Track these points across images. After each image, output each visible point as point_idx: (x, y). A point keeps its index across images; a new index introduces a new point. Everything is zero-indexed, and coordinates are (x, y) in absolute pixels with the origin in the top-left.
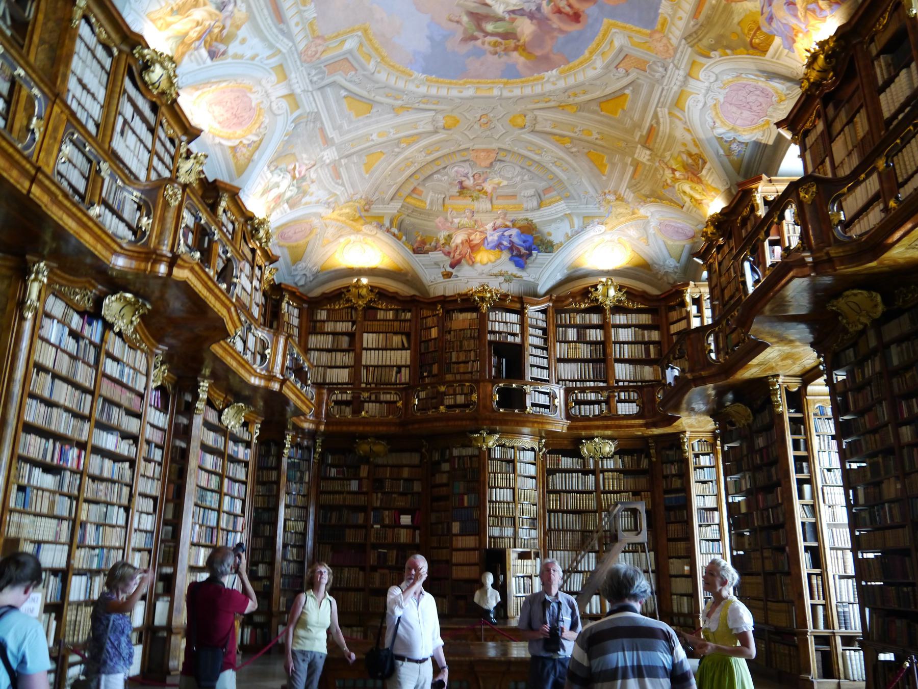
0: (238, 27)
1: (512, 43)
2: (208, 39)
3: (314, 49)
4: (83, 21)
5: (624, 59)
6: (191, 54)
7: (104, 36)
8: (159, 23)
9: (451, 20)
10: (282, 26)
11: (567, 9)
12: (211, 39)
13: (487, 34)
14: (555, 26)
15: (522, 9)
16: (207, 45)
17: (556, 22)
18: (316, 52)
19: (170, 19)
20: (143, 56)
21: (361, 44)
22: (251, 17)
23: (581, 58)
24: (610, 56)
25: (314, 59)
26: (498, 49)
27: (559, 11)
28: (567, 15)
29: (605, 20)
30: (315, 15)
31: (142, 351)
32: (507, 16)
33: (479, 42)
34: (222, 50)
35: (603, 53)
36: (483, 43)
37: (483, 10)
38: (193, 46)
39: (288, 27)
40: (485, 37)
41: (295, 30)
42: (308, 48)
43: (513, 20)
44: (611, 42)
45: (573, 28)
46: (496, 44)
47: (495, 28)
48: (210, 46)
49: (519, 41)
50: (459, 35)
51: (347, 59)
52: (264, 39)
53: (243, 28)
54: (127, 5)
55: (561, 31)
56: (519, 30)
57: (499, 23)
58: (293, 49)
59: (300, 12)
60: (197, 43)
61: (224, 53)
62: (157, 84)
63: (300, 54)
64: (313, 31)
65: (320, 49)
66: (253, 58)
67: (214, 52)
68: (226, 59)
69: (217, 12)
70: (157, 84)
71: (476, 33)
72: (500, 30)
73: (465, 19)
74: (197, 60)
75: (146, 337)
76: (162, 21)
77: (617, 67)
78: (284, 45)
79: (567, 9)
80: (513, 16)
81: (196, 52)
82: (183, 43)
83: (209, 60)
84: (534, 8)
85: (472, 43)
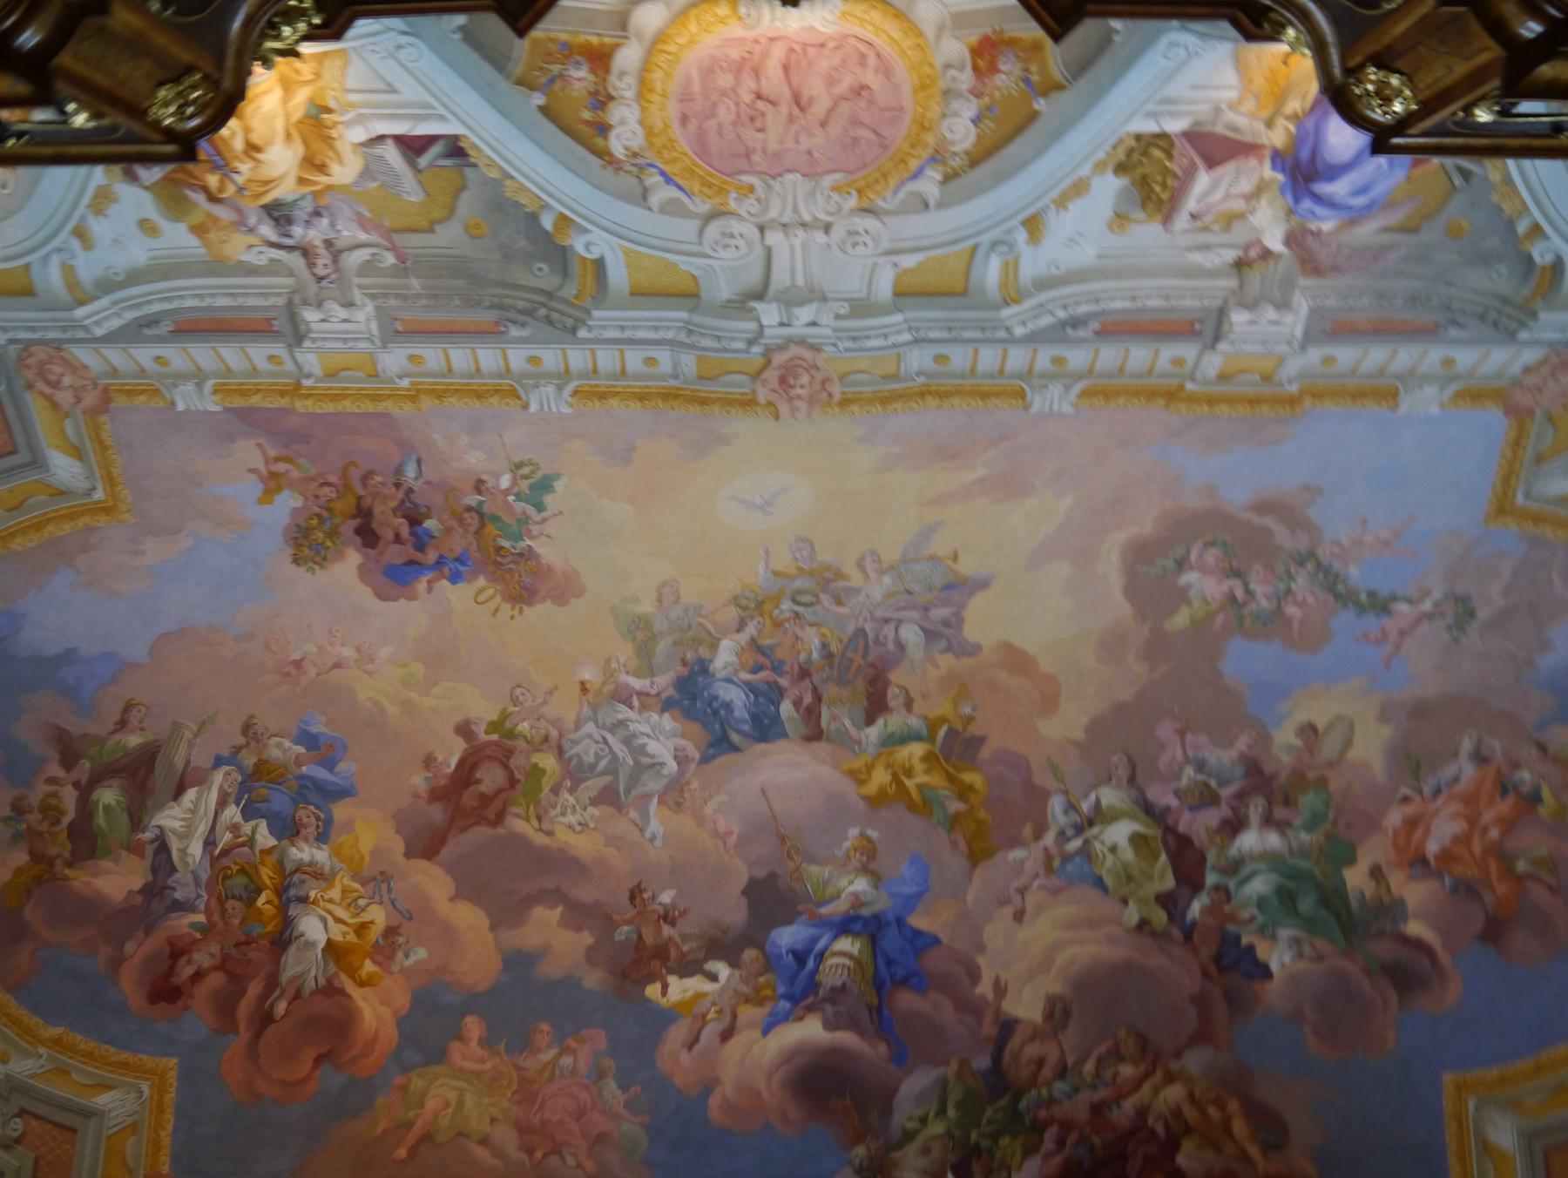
0: (199, 230)
1: (60, 847)
3: (67, 381)
5: (57, 1125)
9: (128, 708)
10: (165, 328)
11: (186, 971)
13: (85, 792)
14: (129, 947)
15: (174, 870)
17: (139, 950)
18: (56, 385)
21: (61, 493)
22: (217, 266)
23: (35, 1021)
24: (60, 1090)
25: (30, 375)
26: (34, 817)
27: (177, 951)
28: (171, 972)
29: (174, 1061)
30: (181, 407)
32: (148, 835)
33: (55, 770)
35: (62, 1071)
36: (52, 780)
37: (161, 779)
39: (159, 339)
40: (76, 785)
41: (144, 355)
42: (75, 368)
43: (137, 849)
44: (107, 1087)
45: (130, 987)
46: (50, 810)
47: (107, 808)
49: (70, 865)
50: (74, 724)
51: (14, 452)
52: (135, 277)
53: (192, 241)
55: (117, 962)
56: (105, 864)
57: (124, 819)
58: (81, 335)
59: (199, 376)
63: (58, 345)
64: (130, 393)
65: (65, 398)
66: (80, 233)
69: (267, 199)
71: (86, 764)
72: (101, 820)
73: (134, 740)
77: (22, 1113)
78: (101, 315)
79: (186, 971)
80: (150, 850)
84: (178, 895)
85: (54, 755)
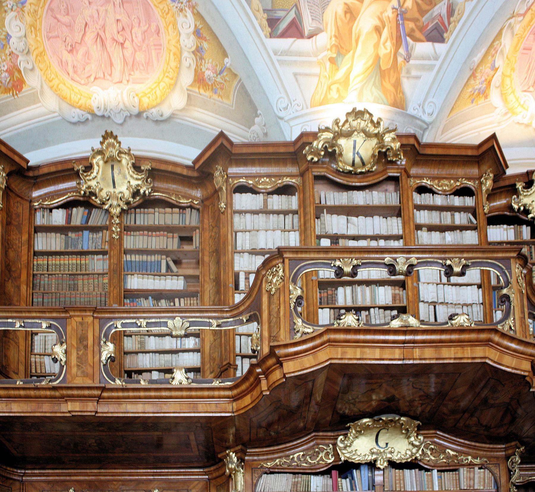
2: (411, 25)
4: (237, 197)
6: (408, 72)
7: (266, 184)
8: (334, 94)
12: (415, 20)
16: (418, 34)
19: (340, 75)
20: (316, 153)
31: (471, 465)
34: (444, 12)
38: (400, 60)
48: (422, 29)
54: (281, 122)
60: (402, 51)
61: (451, 12)
62: (357, 160)
67: (436, 28)
68: (461, 14)
70: (357, 160)
74: (423, 68)
75: (468, 446)
76: (334, 87)
81: (412, 62)
82: (382, 74)
83: (437, 45)
